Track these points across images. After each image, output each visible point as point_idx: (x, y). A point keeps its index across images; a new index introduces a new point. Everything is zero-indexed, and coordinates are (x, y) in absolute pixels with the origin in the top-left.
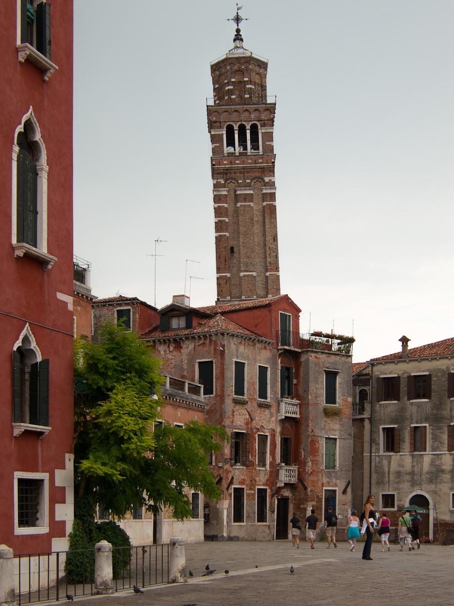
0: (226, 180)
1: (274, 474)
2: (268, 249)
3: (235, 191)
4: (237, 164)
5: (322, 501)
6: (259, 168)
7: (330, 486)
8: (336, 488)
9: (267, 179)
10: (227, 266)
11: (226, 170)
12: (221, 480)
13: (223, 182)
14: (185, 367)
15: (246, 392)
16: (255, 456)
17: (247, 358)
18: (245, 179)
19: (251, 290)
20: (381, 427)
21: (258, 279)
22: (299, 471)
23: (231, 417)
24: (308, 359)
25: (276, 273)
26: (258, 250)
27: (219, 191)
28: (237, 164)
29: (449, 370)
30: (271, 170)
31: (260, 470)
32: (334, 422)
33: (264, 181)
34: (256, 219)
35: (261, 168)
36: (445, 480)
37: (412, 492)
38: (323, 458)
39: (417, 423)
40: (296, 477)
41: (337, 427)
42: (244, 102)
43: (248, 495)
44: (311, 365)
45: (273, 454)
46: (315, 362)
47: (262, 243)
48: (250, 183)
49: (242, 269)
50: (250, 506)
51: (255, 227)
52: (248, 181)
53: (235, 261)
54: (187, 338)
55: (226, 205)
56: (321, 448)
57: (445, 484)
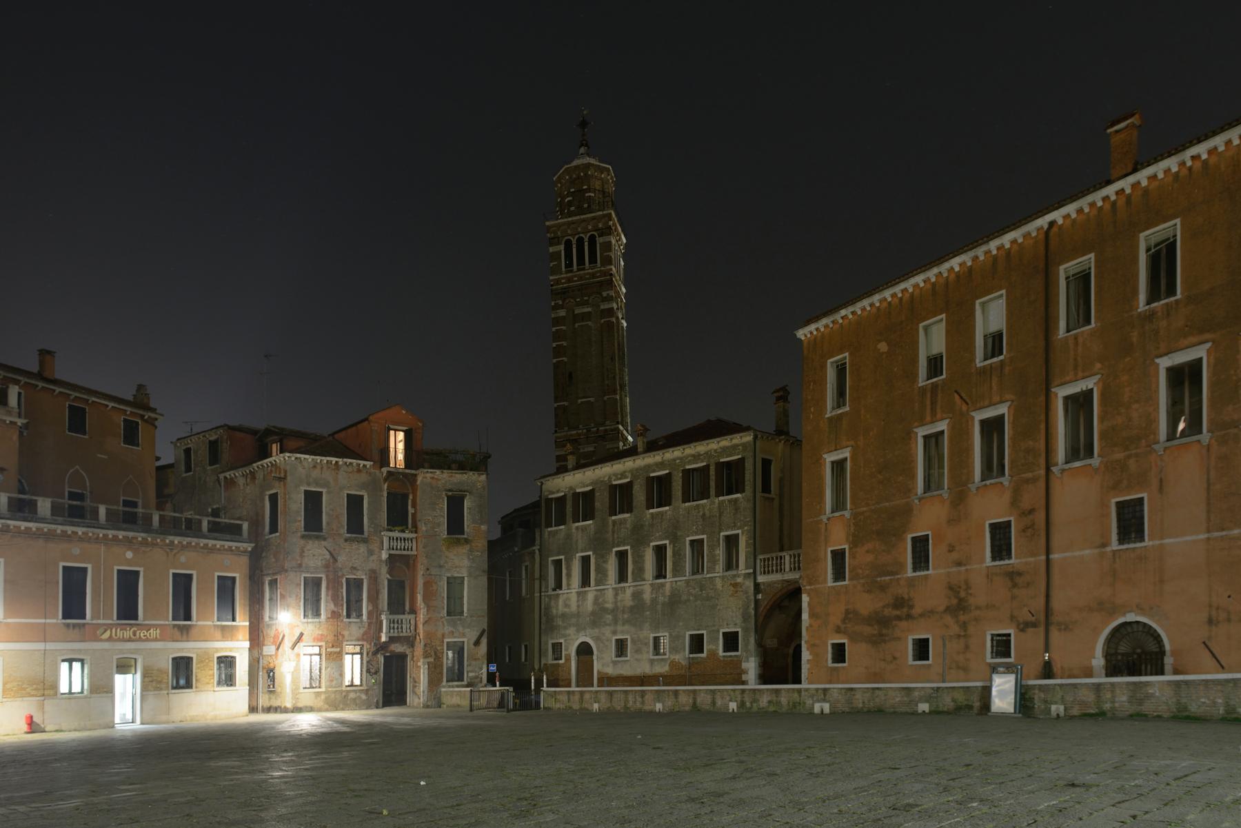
0: (564, 301)
3: (574, 312)
4: (576, 281)
9: (605, 294)
11: (565, 289)
13: (560, 303)
17: (326, 485)
28: (576, 281)
29: (611, 481)
33: (602, 295)
36: (608, 622)
37: (577, 639)
39: (582, 552)
48: (588, 300)
55: (564, 328)
57: (608, 627)
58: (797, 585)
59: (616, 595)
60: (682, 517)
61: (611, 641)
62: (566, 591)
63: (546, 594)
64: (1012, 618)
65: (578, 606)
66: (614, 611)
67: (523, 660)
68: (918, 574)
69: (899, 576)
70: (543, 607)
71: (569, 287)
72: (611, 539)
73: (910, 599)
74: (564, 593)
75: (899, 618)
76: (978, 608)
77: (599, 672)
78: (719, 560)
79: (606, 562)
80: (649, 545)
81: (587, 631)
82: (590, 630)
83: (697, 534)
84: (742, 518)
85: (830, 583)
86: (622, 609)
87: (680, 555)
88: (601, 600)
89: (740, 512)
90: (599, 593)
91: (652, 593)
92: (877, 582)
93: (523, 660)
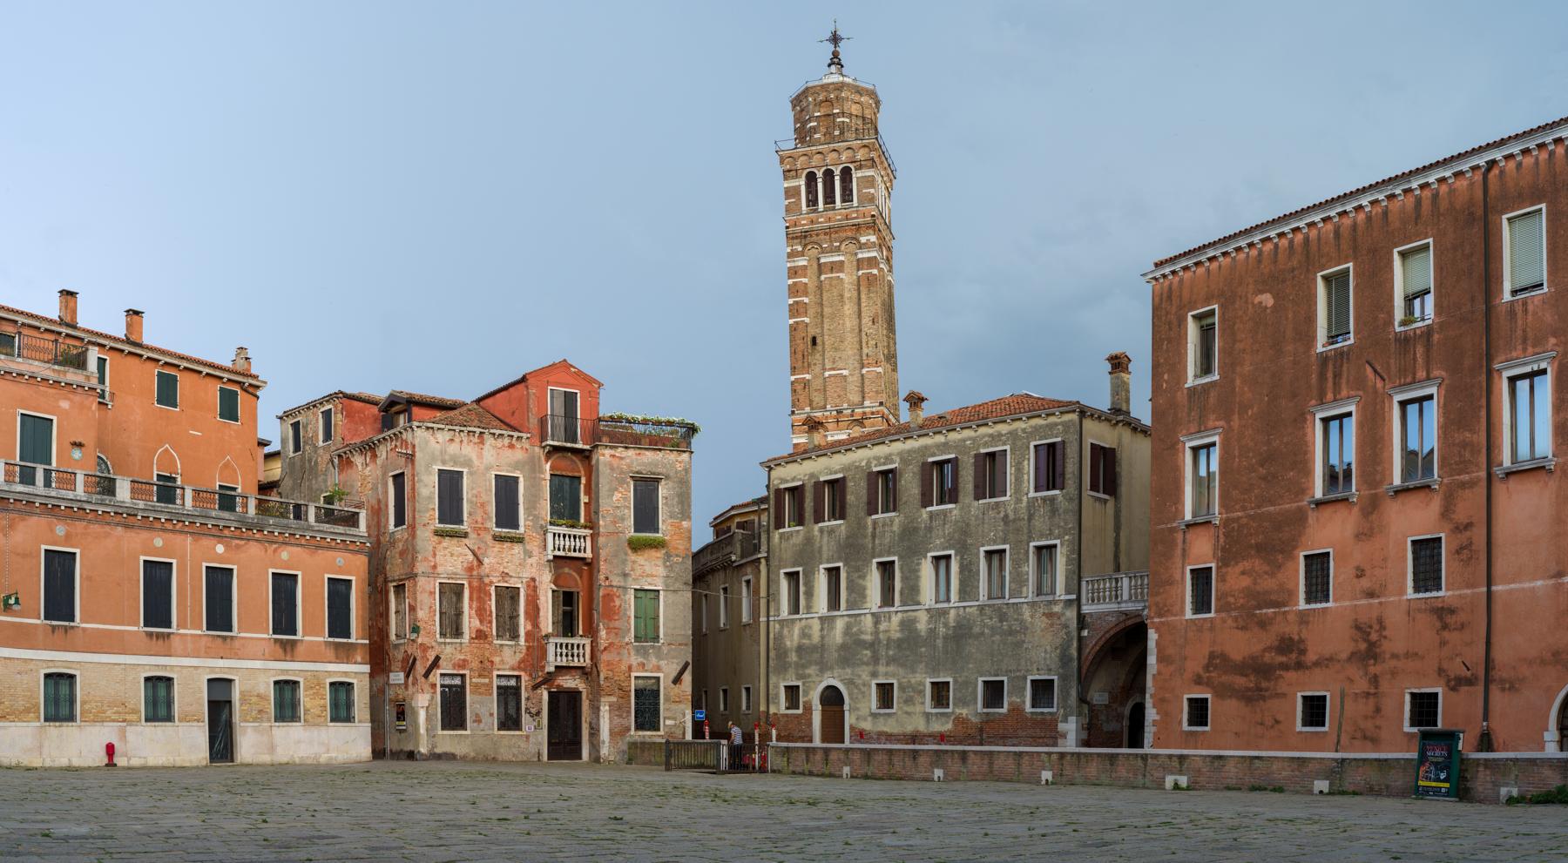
2: (864, 337)
3: (818, 259)
4: (821, 223)
5: (629, 696)
6: (853, 226)
7: (646, 671)
8: (661, 675)
9: (863, 240)
10: (806, 364)
13: (800, 248)
15: (465, 518)
16: (491, 622)
18: (831, 242)
19: (839, 396)
20: (782, 571)
21: (850, 379)
22: (592, 646)
23: (431, 559)
25: (876, 369)
26: (851, 339)
27: (794, 261)
31: (501, 645)
32: (653, 563)
34: (847, 295)
35: (855, 225)
36: (865, 659)
37: (821, 682)
38: (629, 624)
39: (828, 562)
40: (588, 656)
41: (661, 571)
42: (833, 140)
47: (856, 327)
49: (827, 367)
50: (482, 706)
51: (846, 307)
52: (838, 244)
53: (818, 356)
55: (805, 280)
57: (865, 667)
58: (1138, 620)
59: (876, 623)
60: (973, 519)
61: (870, 686)
62: (804, 616)
63: (776, 619)
64: (1441, 671)
65: (822, 637)
66: (872, 645)
67: (744, 707)
68: (1313, 606)
69: (1287, 609)
70: (771, 636)
72: (870, 546)
73: (1301, 641)
74: (802, 619)
75: (1285, 667)
76: (1395, 656)
77: (852, 728)
78: (1028, 580)
79: (863, 577)
80: (926, 557)
81: (835, 671)
82: (840, 670)
83: (995, 543)
84: (1062, 524)
85: (1189, 615)
86: (885, 642)
87: (970, 571)
88: (855, 629)
89: (1059, 515)
90: (852, 620)
91: (929, 622)
92: (1255, 615)
93: (744, 707)
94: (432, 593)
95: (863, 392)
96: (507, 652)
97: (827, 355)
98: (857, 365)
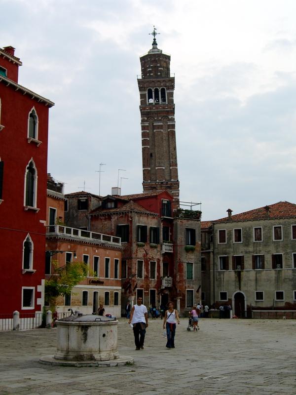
1: (159, 282)
3: (153, 124)
8: (193, 290)
9: (170, 117)
12: (131, 285)
13: (146, 119)
14: (113, 228)
18: (158, 117)
21: (166, 170)
24: (177, 223)
30: (173, 112)
33: (168, 118)
34: (164, 138)
42: (157, 77)
43: (145, 293)
44: (178, 226)
45: (159, 271)
46: (182, 225)
47: (168, 151)
49: (157, 165)
52: (160, 118)
53: (153, 161)
54: (114, 214)
55: (148, 131)
56: (184, 268)
71: (151, 112)
94: (136, 264)
95: (170, 175)
96: (153, 283)
97: (157, 161)
98: (168, 166)
